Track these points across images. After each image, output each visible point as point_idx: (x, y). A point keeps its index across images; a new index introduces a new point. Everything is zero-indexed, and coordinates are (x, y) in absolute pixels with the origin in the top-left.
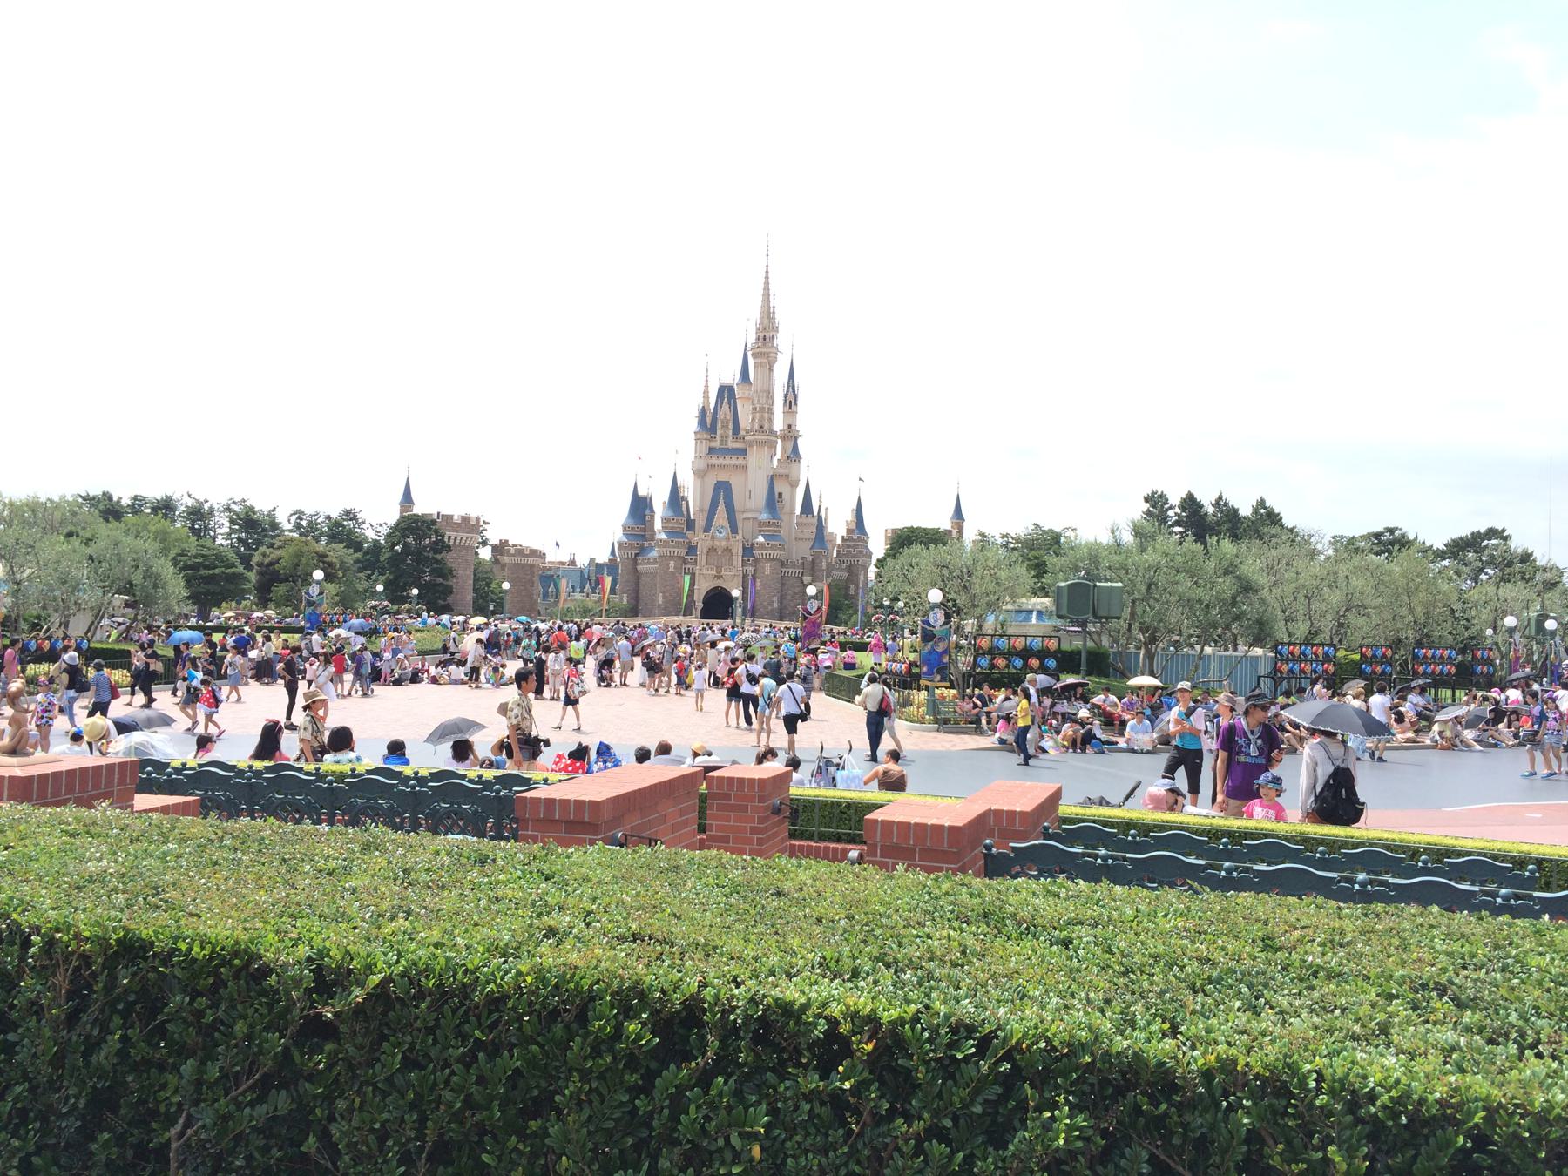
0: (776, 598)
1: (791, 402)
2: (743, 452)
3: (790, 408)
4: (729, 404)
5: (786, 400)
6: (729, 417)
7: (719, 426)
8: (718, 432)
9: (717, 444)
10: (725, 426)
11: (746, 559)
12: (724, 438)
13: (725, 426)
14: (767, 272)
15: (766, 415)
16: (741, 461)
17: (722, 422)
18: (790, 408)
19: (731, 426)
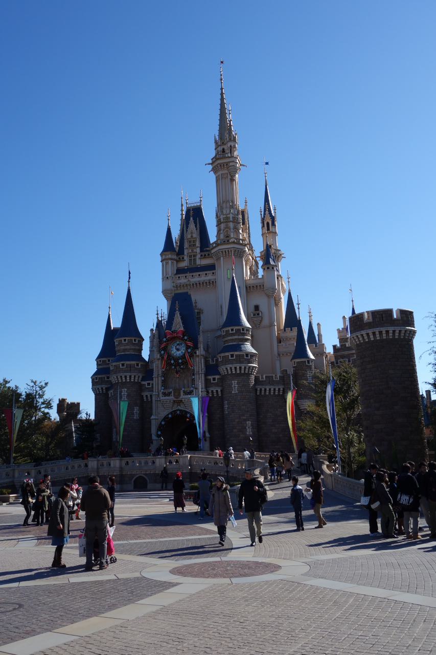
0: (249, 423)
1: (269, 222)
2: (212, 267)
3: (268, 229)
4: (195, 223)
5: (263, 223)
6: (196, 234)
7: (186, 245)
8: (186, 252)
9: (184, 264)
10: (193, 245)
11: (211, 377)
12: (192, 257)
13: (193, 245)
14: (222, 94)
15: (231, 225)
16: (210, 277)
17: (190, 242)
18: (268, 229)
19: (198, 244)
